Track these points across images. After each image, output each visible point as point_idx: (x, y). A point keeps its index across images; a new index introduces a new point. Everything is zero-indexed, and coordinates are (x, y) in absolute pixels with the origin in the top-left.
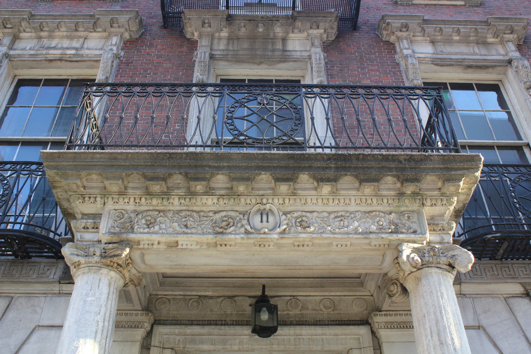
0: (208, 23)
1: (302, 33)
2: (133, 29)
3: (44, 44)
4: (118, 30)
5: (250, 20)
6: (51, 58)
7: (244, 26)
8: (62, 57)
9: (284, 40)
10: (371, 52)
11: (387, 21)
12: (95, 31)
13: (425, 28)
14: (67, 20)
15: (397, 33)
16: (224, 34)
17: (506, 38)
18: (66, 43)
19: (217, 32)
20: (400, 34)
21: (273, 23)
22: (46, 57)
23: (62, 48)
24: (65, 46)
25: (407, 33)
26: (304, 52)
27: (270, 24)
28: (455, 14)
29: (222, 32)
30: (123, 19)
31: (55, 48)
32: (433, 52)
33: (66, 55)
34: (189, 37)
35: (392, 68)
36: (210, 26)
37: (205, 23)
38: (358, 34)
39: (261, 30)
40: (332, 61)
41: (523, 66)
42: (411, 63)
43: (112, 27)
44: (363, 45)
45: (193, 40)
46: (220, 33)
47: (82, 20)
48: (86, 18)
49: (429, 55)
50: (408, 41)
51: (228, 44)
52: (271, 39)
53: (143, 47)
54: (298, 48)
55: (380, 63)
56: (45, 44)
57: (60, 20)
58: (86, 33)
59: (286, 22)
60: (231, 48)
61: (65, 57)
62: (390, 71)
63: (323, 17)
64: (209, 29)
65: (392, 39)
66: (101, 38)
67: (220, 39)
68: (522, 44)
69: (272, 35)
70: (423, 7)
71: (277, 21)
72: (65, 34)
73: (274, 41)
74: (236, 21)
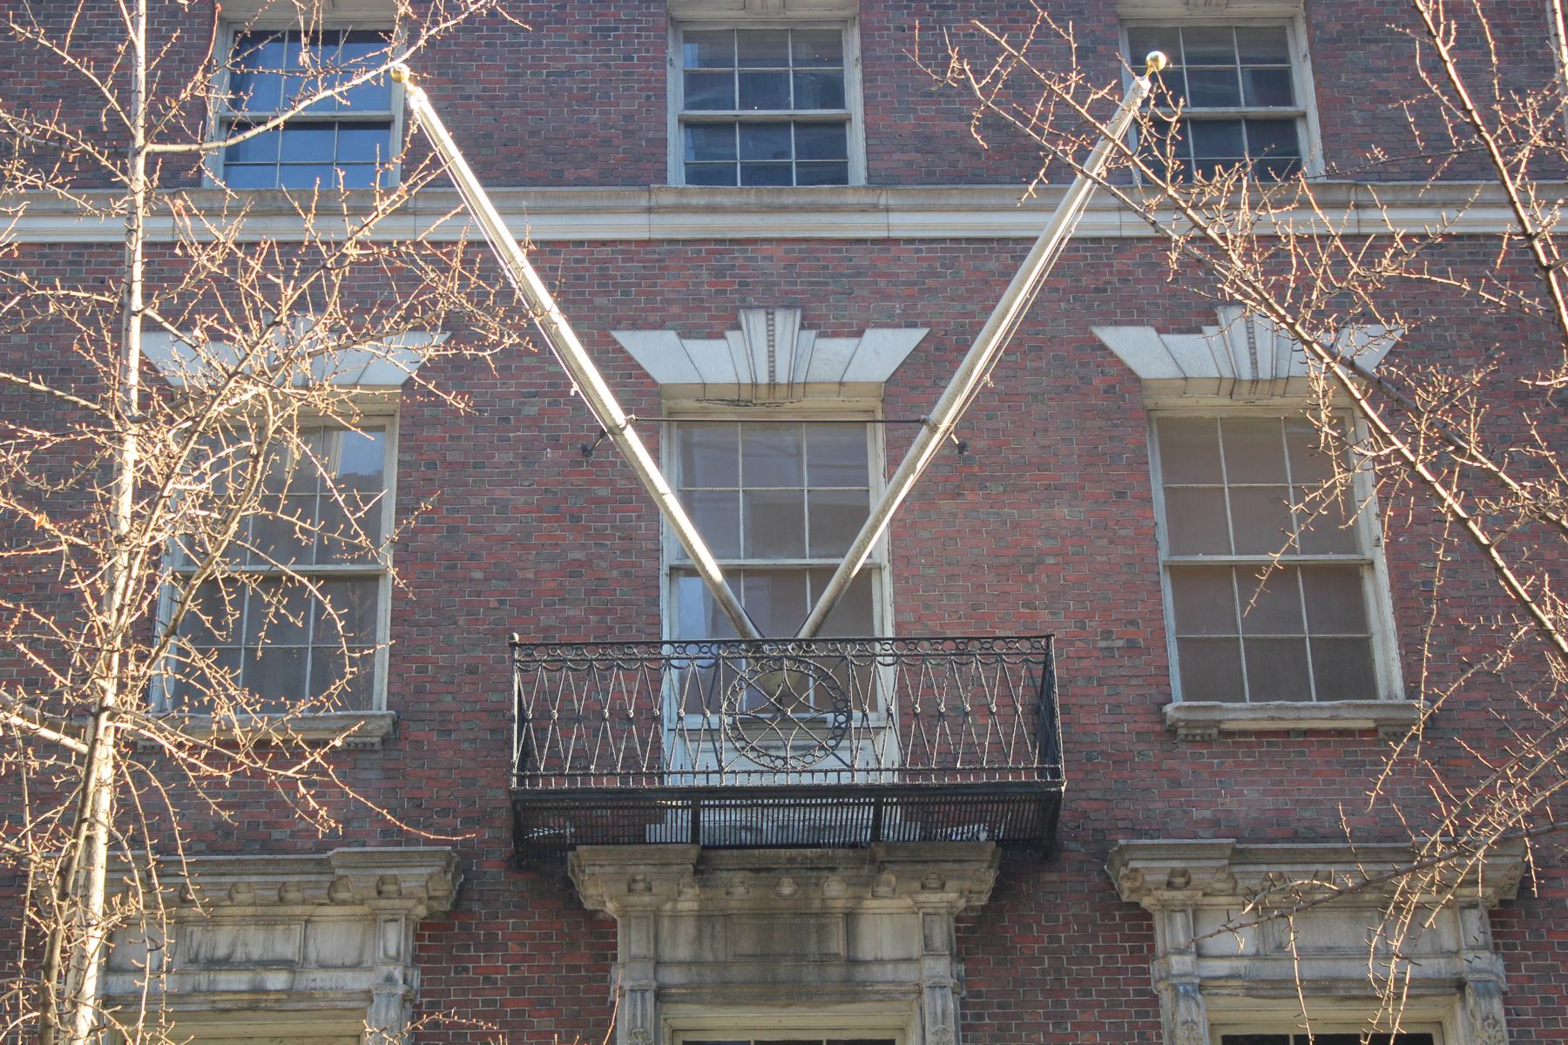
0: (644, 880)
1: (899, 897)
2: (438, 894)
3: (195, 945)
4: (397, 903)
5: (757, 870)
6: (228, 1006)
7: (743, 883)
8: (258, 1001)
9: (851, 917)
10: (1085, 949)
11: (1133, 864)
12: (333, 902)
13: (1237, 876)
14: (254, 879)
15: (1159, 892)
16: (688, 903)
17: (1464, 896)
18: (256, 943)
19: (668, 900)
20: (1168, 895)
21: (819, 878)
22: (214, 1002)
23: (250, 964)
24: (256, 953)
25: (1188, 893)
26: (904, 967)
27: (813, 881)
28: (1342, 774)
29: (682, 898)
30: (414, 878)
31: (226, 963)
32: (1252, 950)
33: (267, 992)
34: (591, 908)
35: (1138, 1015)
36: (650, 889)
37: (634, 881)
38: (1054, 877)
39: (787, 890)
40: (978, 995)
41: (1487, 1018)
42: (1183, 1019)
43: (380, 893)
44: (1066, 925)
45: (601, 916)
46: (676, 901)
47: (296, 878)
48: (306, 869)
49: (1241, 965)
50: (1187, 917)
51: (699, 939)
52: (816, 914)
53: (467, 948)
54: (888, 952)
55: (1107, 993)
56: (199, 945)
57: (234, 879)
58: (308, 909)
59: (854, 872)
60: (708, 955)
61: (266, 1001)
62: (1132, 1025)
63: (955, 861)
64: (647, 899)
65: (1146, 902)
66: (350, 919)
67: (676, 916)
68: (1514, 898)
69: (817, 904)
70: (1249, 745)
71: (832, 869)
72: (250, 910)
73: (824, 921)
74: (719, 874)
